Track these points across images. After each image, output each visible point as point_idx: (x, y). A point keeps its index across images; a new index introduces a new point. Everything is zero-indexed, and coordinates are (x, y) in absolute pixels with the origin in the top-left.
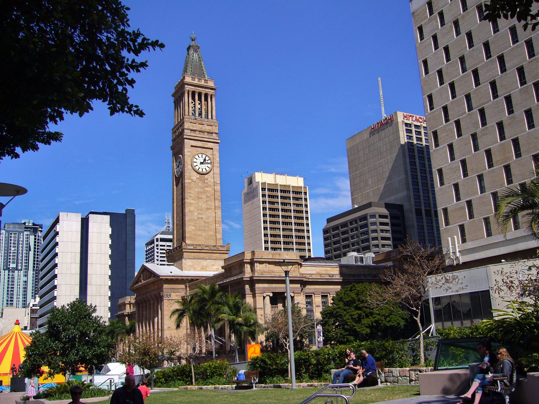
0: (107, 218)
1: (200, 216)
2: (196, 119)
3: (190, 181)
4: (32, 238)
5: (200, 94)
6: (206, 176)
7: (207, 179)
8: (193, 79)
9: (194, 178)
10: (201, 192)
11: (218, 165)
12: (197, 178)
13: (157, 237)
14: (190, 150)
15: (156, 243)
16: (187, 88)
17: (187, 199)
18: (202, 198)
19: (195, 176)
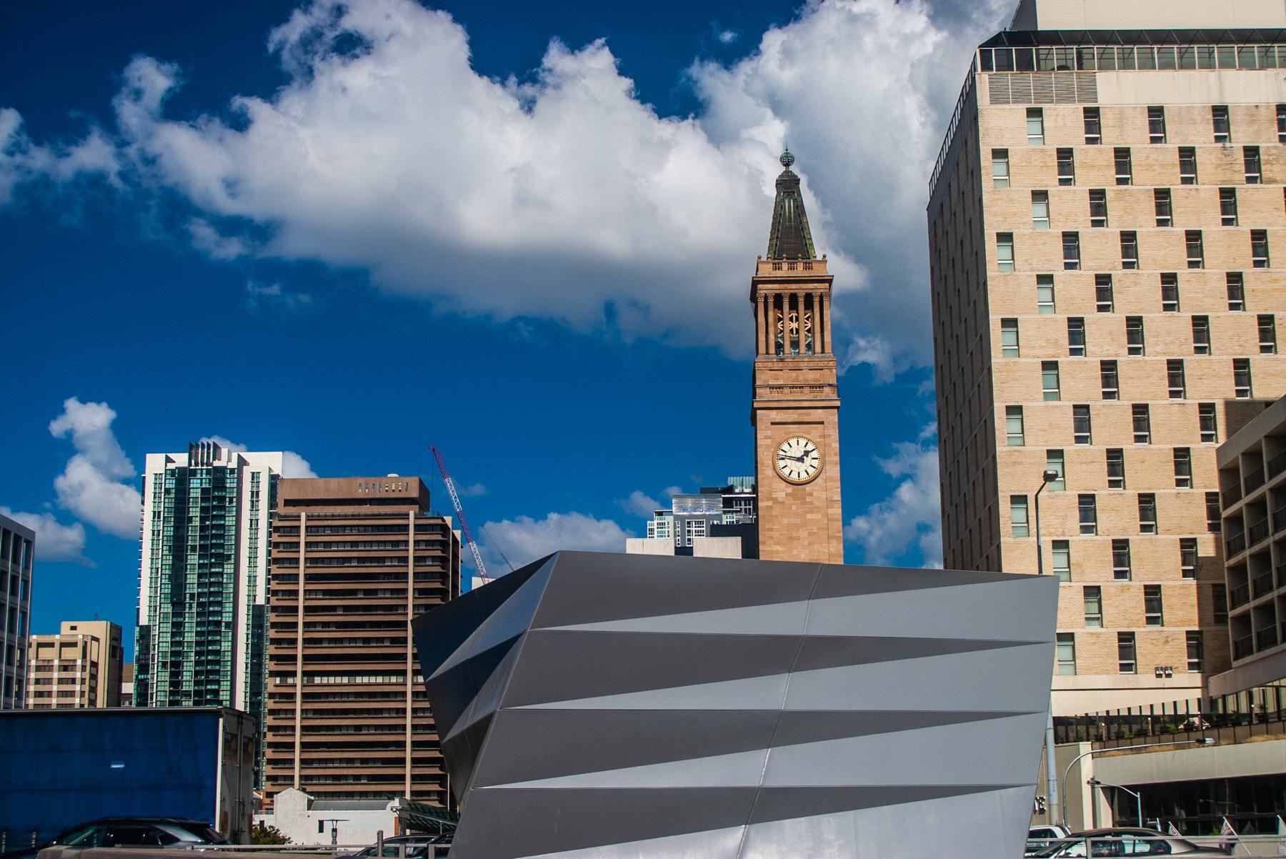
2: (782, 360)
3: (770, 503)
5: (793, 299)
6: (808, 488)
7: (811, 494)
8: (777, 267)
9: (781, 496)
10: (797, 526)
11: (837, 458)
12: (787, 495)
14: (769, 433)
16: (763, 289)
17: (764, 543)
18: (799, 539)
19: (781, 491)
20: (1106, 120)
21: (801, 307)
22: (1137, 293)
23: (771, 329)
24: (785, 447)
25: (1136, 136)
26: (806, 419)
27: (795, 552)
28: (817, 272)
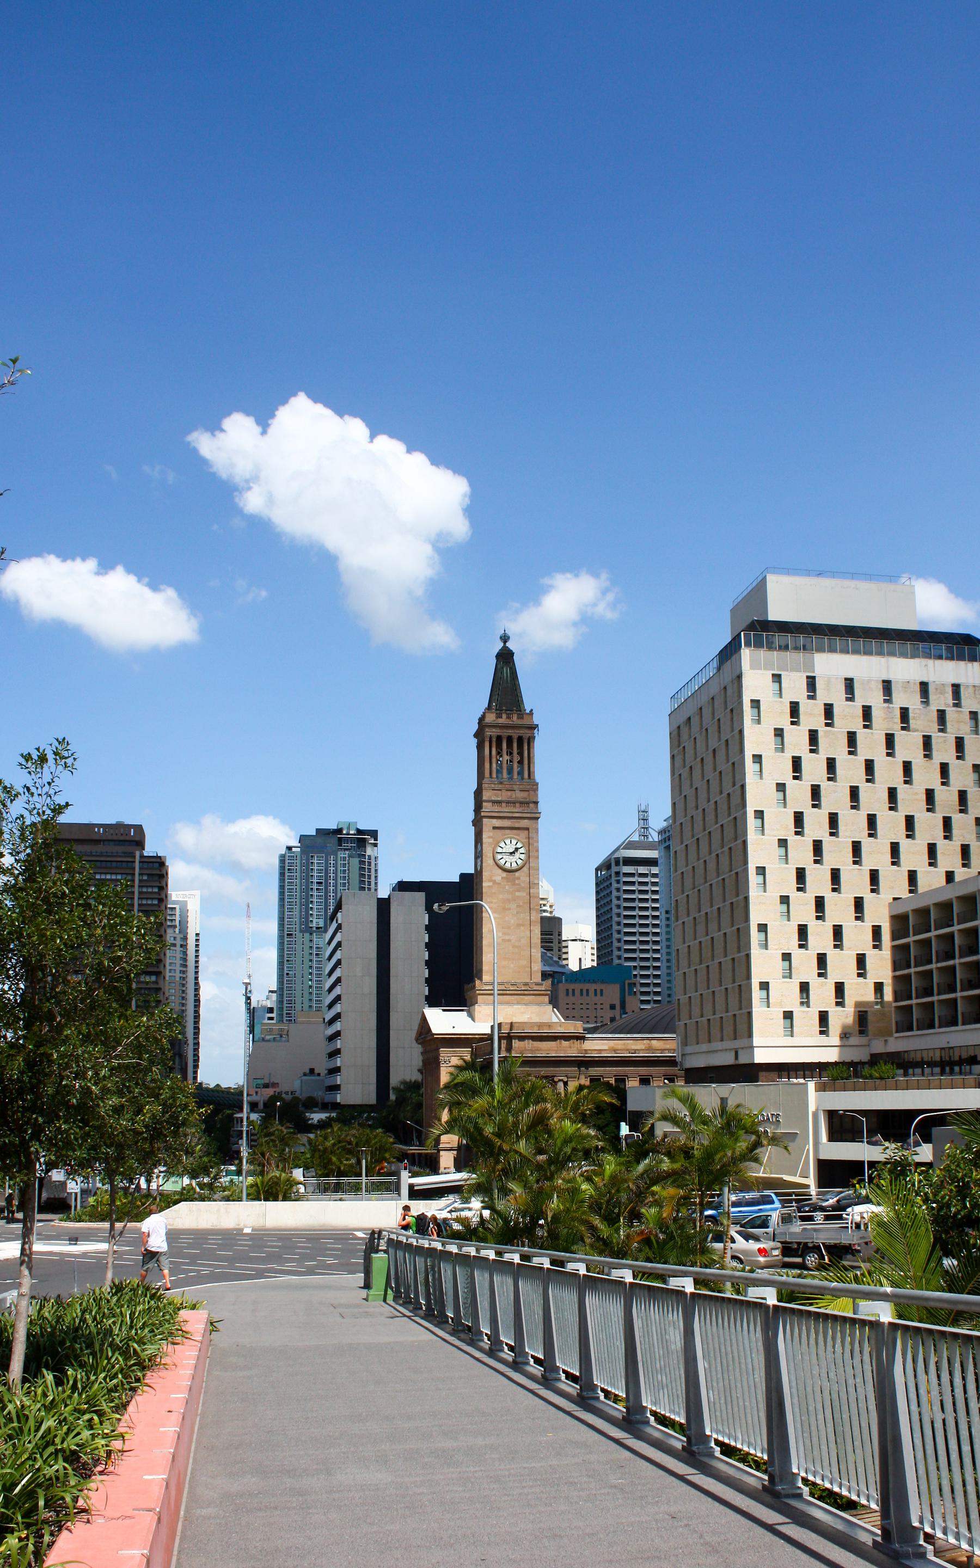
0: (420, 897)
1: (507, 937)
2: (501, 783)
4: (355, 862)
5: (510, 739)
6: (517, 874)
7: (519, 878)
9: (498, 879)
13: (616, 855)
15: (614, 869)
16: (489, 732)
19: (499, 875)
20: (819, 685)
21: (515, 745)
22: (836, 797)
23: (494, 760)
24: (502, 844)
25: (837, 696)
26: (517, 825)
27: (507, 919)
28: (526, 722)
